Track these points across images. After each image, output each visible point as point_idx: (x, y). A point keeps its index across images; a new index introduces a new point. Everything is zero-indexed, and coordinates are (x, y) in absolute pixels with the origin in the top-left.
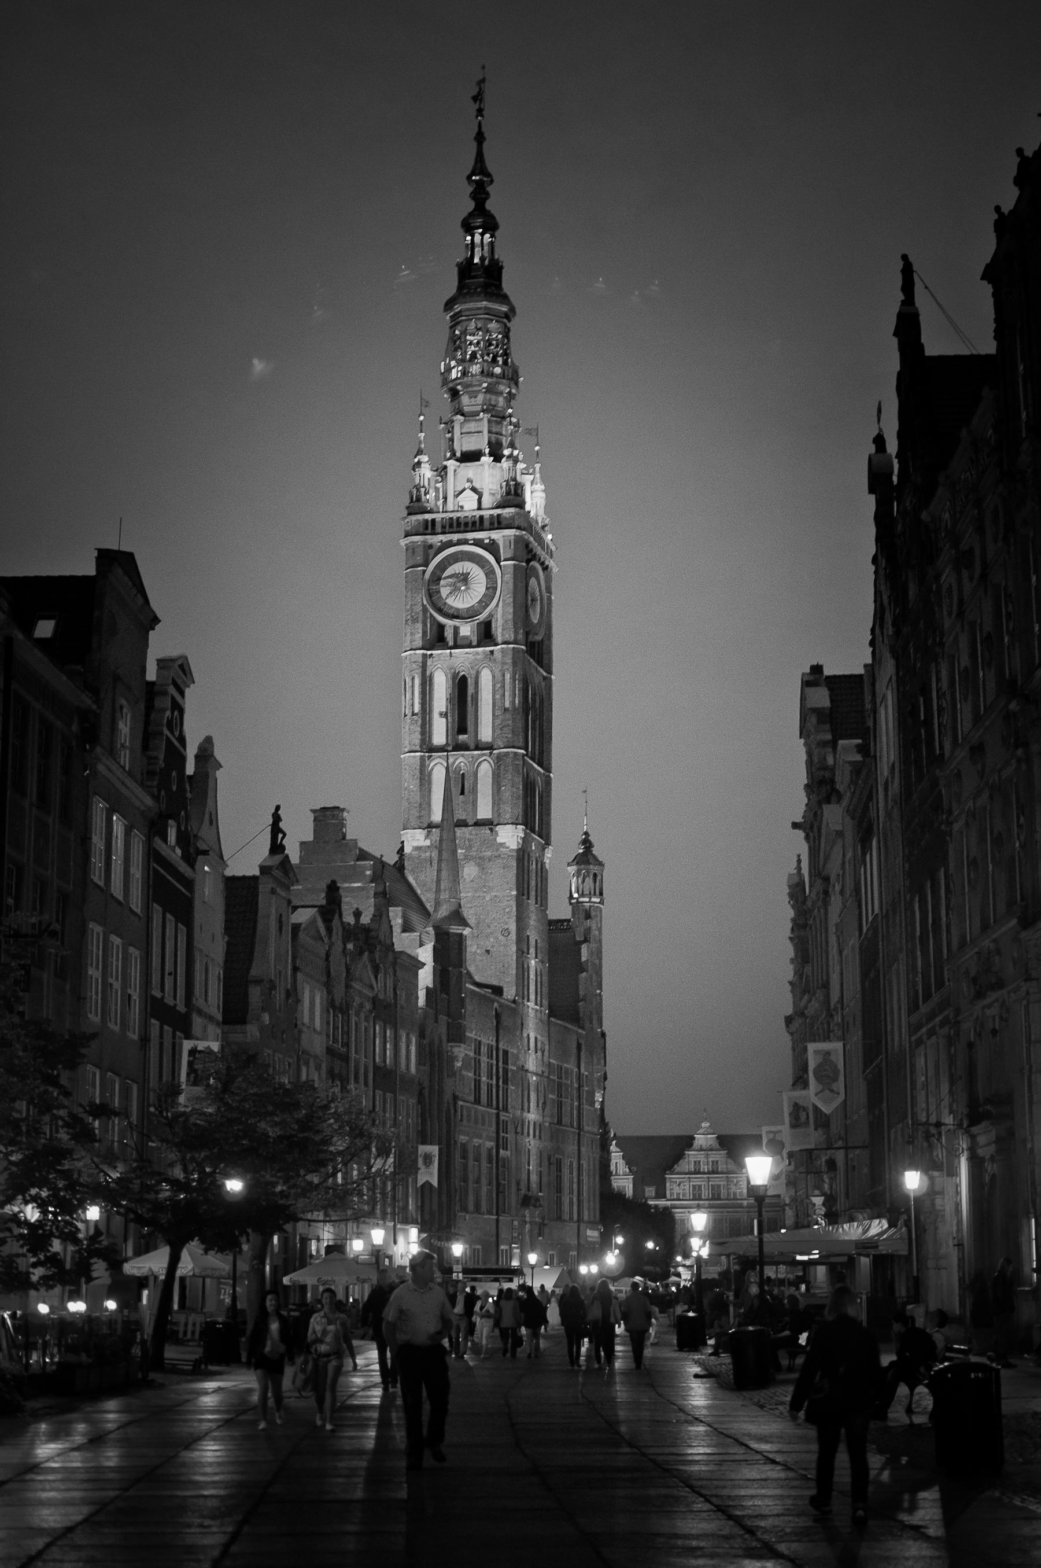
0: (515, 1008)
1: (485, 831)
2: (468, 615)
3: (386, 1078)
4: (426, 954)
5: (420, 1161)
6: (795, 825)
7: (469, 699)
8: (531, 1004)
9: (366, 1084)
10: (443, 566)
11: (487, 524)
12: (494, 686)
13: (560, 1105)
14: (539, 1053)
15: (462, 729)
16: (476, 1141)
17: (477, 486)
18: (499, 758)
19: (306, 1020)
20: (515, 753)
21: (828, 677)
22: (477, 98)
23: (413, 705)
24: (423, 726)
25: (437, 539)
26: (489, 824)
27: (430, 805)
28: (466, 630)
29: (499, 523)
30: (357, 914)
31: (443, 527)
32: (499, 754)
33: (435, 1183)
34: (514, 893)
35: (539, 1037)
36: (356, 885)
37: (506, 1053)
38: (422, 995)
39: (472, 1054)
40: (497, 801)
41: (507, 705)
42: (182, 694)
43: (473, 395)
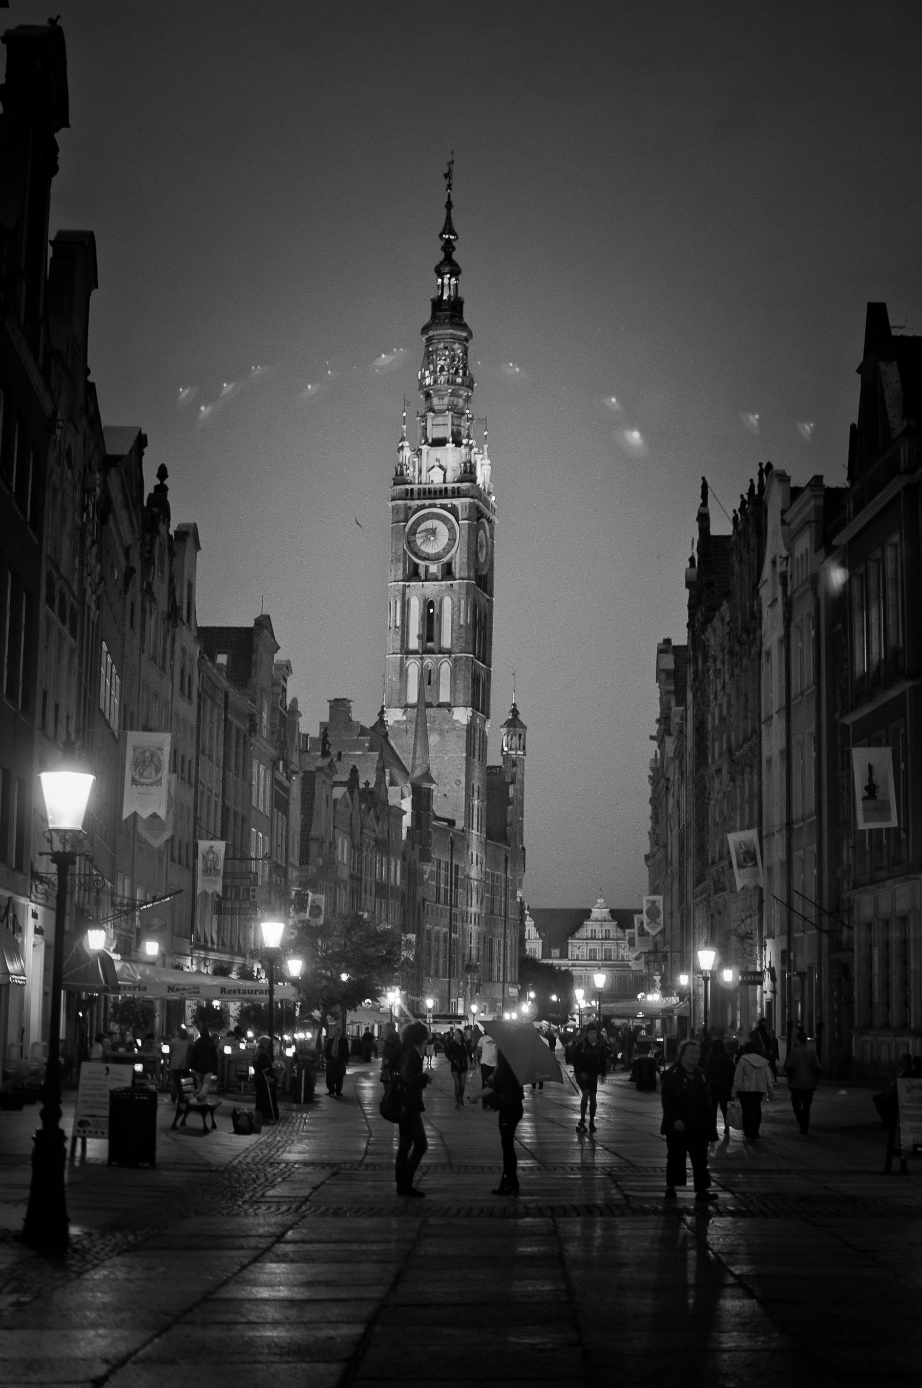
0: (463, 836)
2: (436, 558)
3: (382, 889)
4: (406, 805)
6: (652, 738)
8: (474, 832)
10: (418, 523)
11: (450, 493)
12: (452, 609)
13: (493, 901)
14: (479, 866)
15: (430, 639)
16: (437, 928)
17: (443, 464)
18: (455, 660)
19: (340, 859)
21: (675, 647)
22: (447, 175)
23: (395, 621)
24: (403, 636)
26: (448, 706)
27: (406, 691)
28: (434, 568)
29: (459, 493)
30: (367, 784)
31: (419, 494)
34: (464, 755)
36: (358, 753)
37: (457, 867)
38: (404, 831)
39: (435, 869)
40: (453, 691)
41: (462, 622)
42: (286, 681)
43: (441, 397)
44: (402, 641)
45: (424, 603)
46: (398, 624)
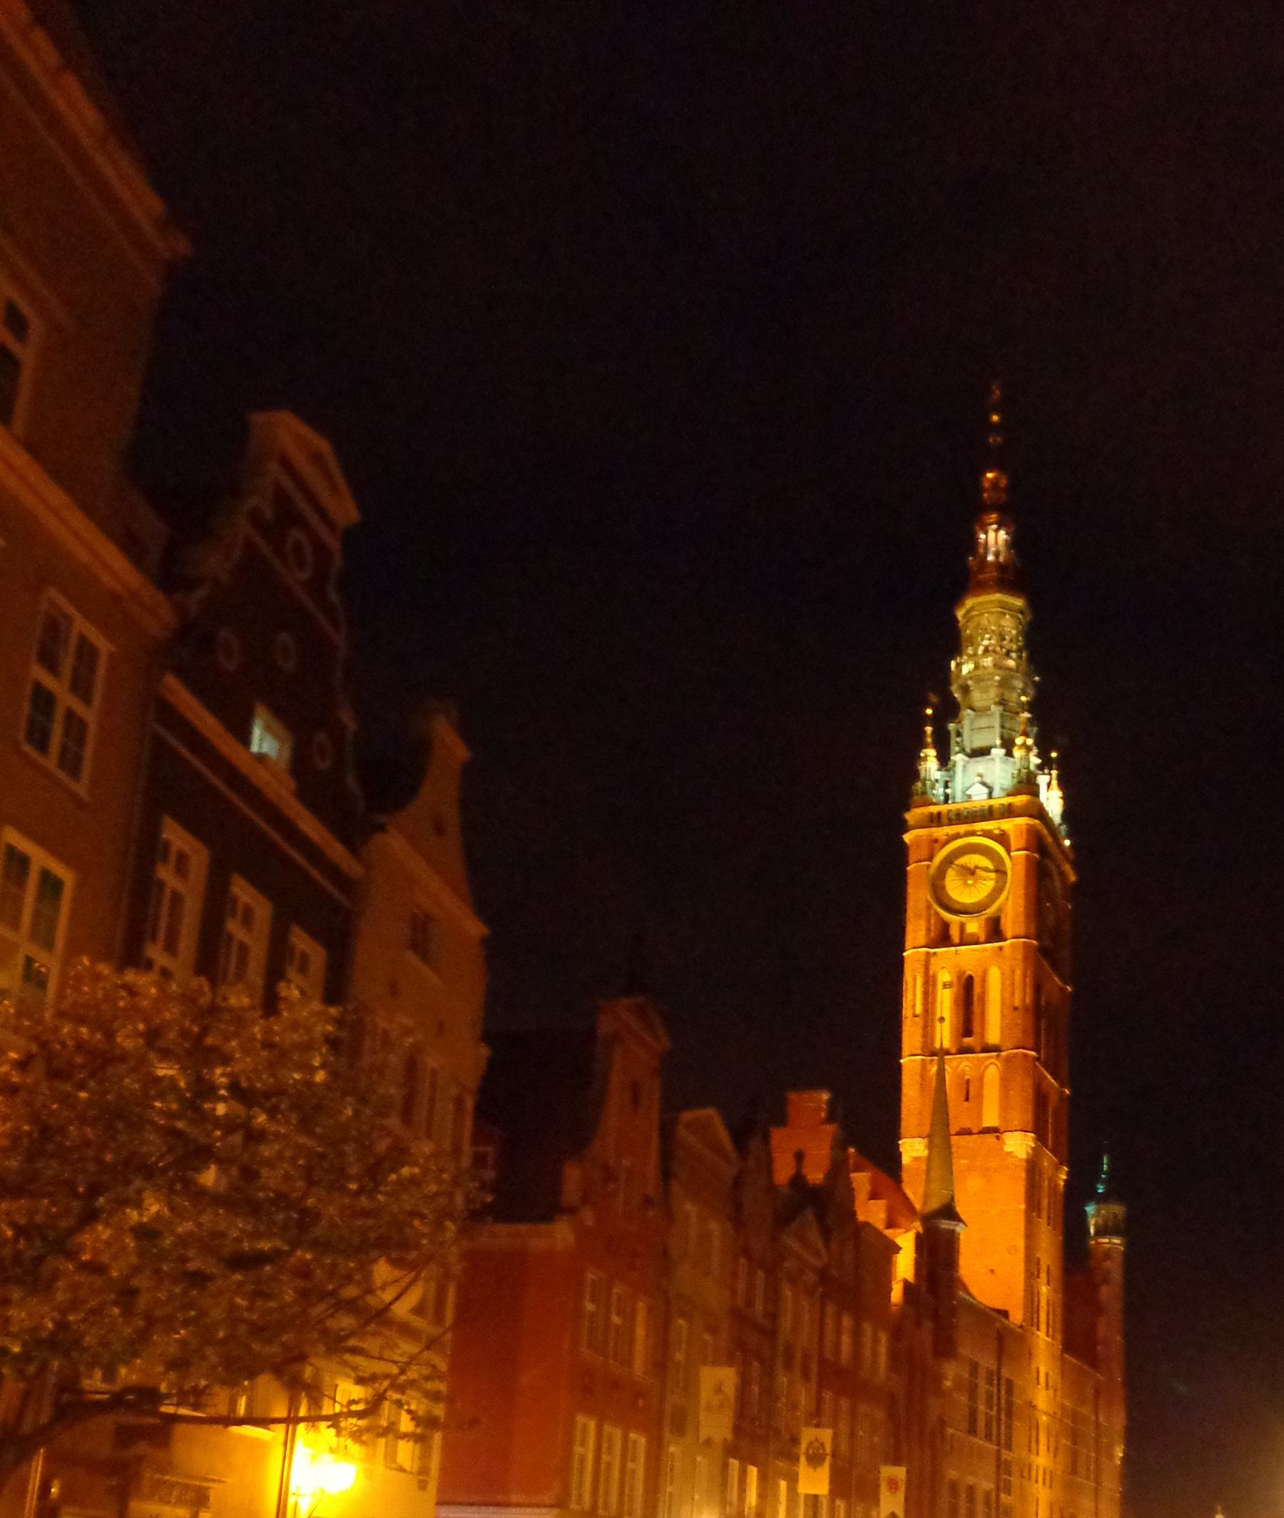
1: (990, 1138)
4: (906, 1242)
7: (975, 998)
8: (1041, 1334)
10: (949, 861)
12: (1003, 984)
14: (1051, 1392)
15: (967, 1032)
16: (970, 1480)
17: (988, 781)
18: (1008, 1060)
20: (1026, 1055)
23: (914, 1006)
24: (925, 1027)
25: (942, 832)
28: (974, 926)
31: (950, 819)
32: (1007, 1056)
34: (1023, 1206)
35: (1051, 1374)
40: (1005, 1106)
43: (985, 690)
44: (925, 1035)
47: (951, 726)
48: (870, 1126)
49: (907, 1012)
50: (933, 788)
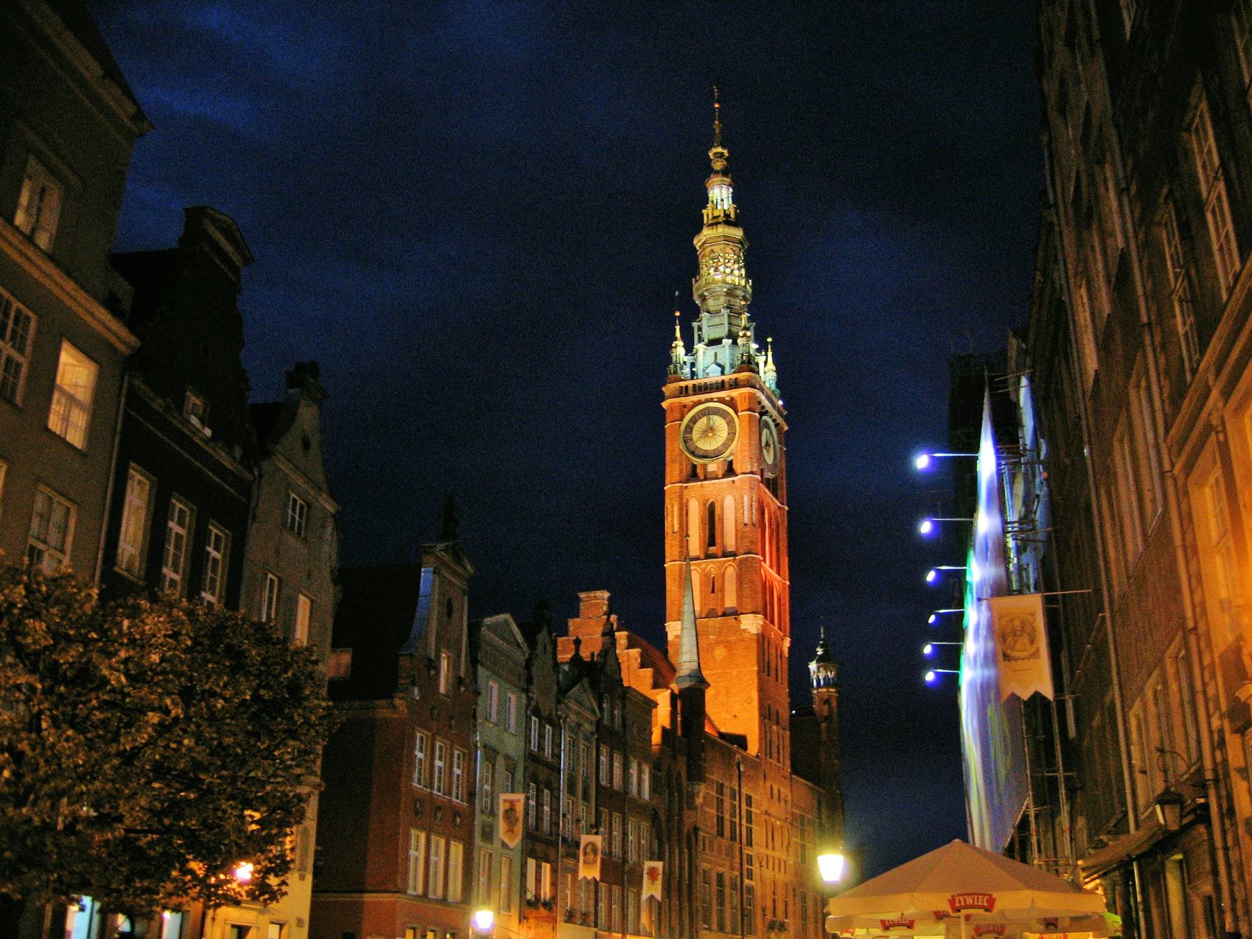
1: (731, 619)
4: (663, 699)
5: (645, 877)
9: (586, 797)
10: (694, 421)
11: (727, 386)
14: (783, 804)
15: (712, 541)
18: (741, 562)
33: (659, 897)
34: (756, 669)
37: (749, 798)
40: (740, 597)
41: (746, 520)
43: (716, 298)
44: (681, 547)
45: (704, 505)
46: (676, 528)
47: (695, 324)
48: (644, 615)
49: (668, 529)
50: (682, 368)
